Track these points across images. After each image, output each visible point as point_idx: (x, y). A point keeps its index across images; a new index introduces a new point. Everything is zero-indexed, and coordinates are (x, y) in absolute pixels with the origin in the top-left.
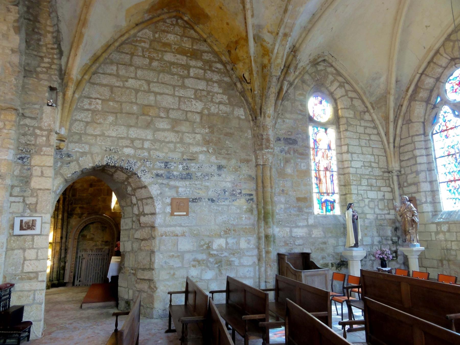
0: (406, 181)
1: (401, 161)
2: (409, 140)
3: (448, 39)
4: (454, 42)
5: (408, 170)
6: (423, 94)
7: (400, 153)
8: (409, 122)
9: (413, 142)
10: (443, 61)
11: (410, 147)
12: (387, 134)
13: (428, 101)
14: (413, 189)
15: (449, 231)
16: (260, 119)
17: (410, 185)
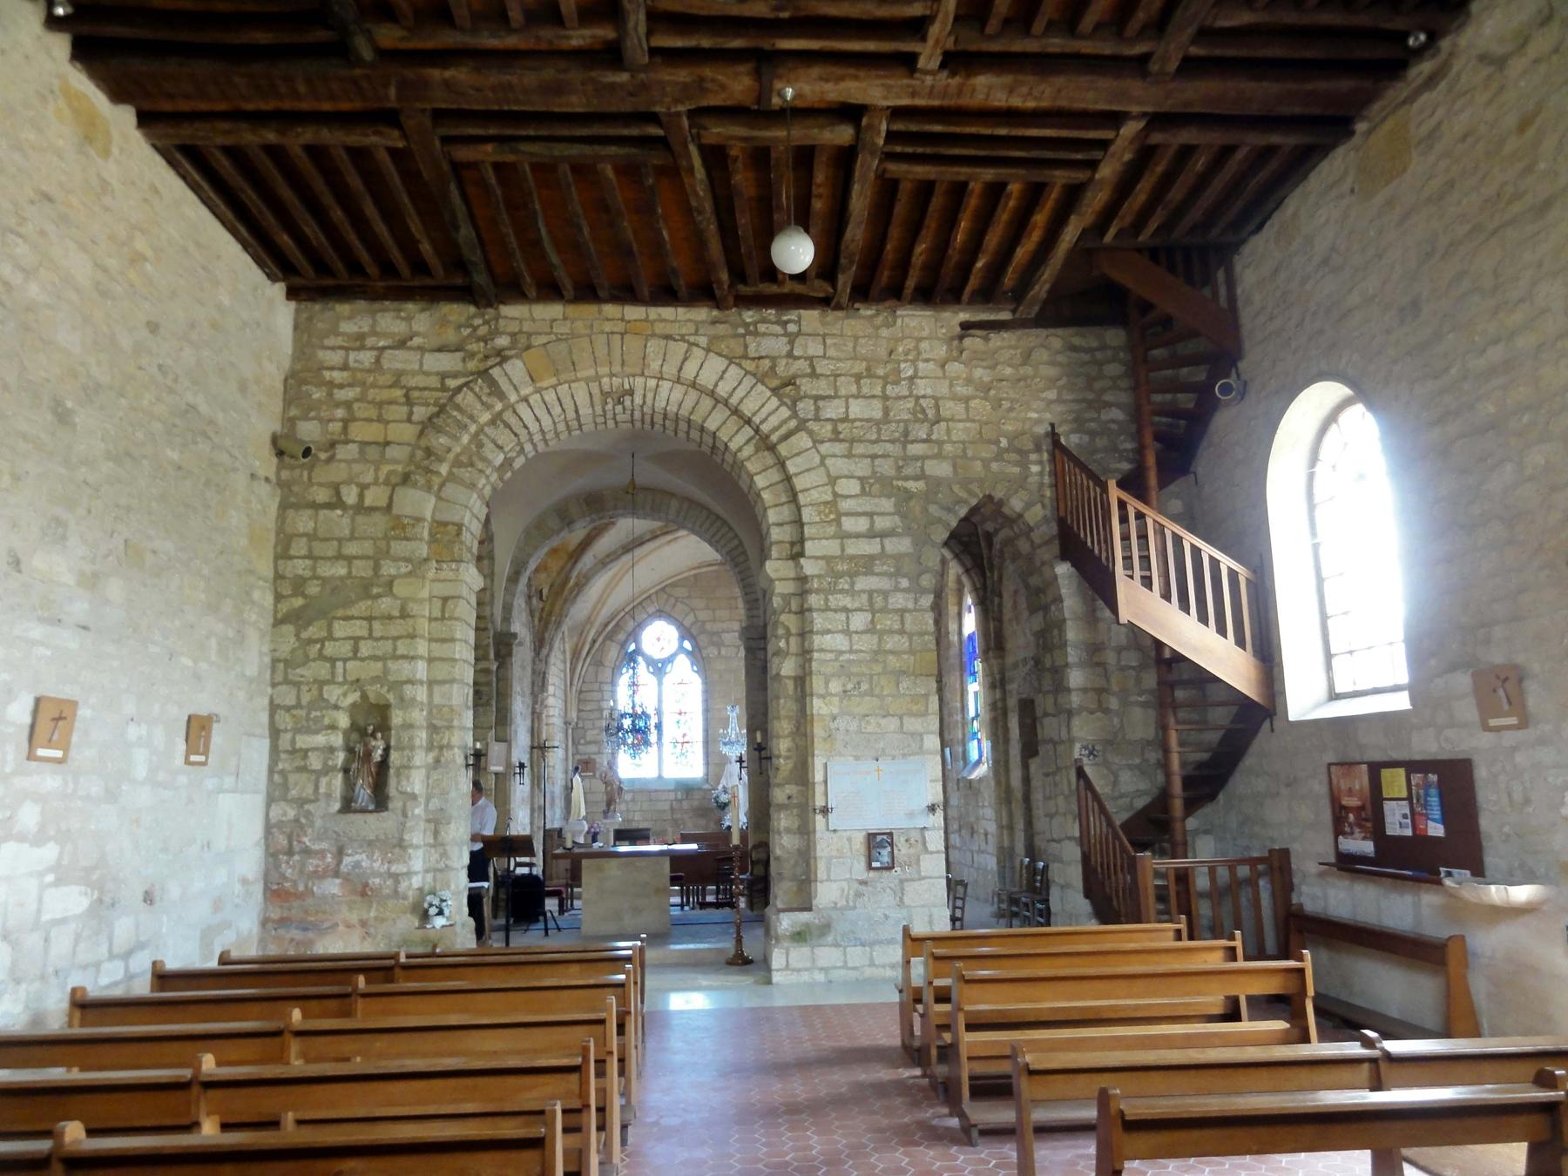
0: (584, 737)
1: (579, 711)
2: (596, 687)
3: (663, 589)
4: (670, 596)
5: (588, 724)
6: (621, 637)
7: (579, 700)
8: (599, 664)
9: (600, 690)
10: (651, 610)
11: (596, 696)
12: (573, 670)
13: (624, 645)
14: (592, 748)
15: (633, 800)
16: (545, 651)
17: (590, 743)
